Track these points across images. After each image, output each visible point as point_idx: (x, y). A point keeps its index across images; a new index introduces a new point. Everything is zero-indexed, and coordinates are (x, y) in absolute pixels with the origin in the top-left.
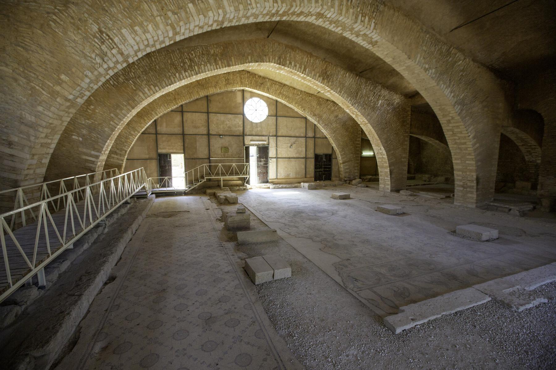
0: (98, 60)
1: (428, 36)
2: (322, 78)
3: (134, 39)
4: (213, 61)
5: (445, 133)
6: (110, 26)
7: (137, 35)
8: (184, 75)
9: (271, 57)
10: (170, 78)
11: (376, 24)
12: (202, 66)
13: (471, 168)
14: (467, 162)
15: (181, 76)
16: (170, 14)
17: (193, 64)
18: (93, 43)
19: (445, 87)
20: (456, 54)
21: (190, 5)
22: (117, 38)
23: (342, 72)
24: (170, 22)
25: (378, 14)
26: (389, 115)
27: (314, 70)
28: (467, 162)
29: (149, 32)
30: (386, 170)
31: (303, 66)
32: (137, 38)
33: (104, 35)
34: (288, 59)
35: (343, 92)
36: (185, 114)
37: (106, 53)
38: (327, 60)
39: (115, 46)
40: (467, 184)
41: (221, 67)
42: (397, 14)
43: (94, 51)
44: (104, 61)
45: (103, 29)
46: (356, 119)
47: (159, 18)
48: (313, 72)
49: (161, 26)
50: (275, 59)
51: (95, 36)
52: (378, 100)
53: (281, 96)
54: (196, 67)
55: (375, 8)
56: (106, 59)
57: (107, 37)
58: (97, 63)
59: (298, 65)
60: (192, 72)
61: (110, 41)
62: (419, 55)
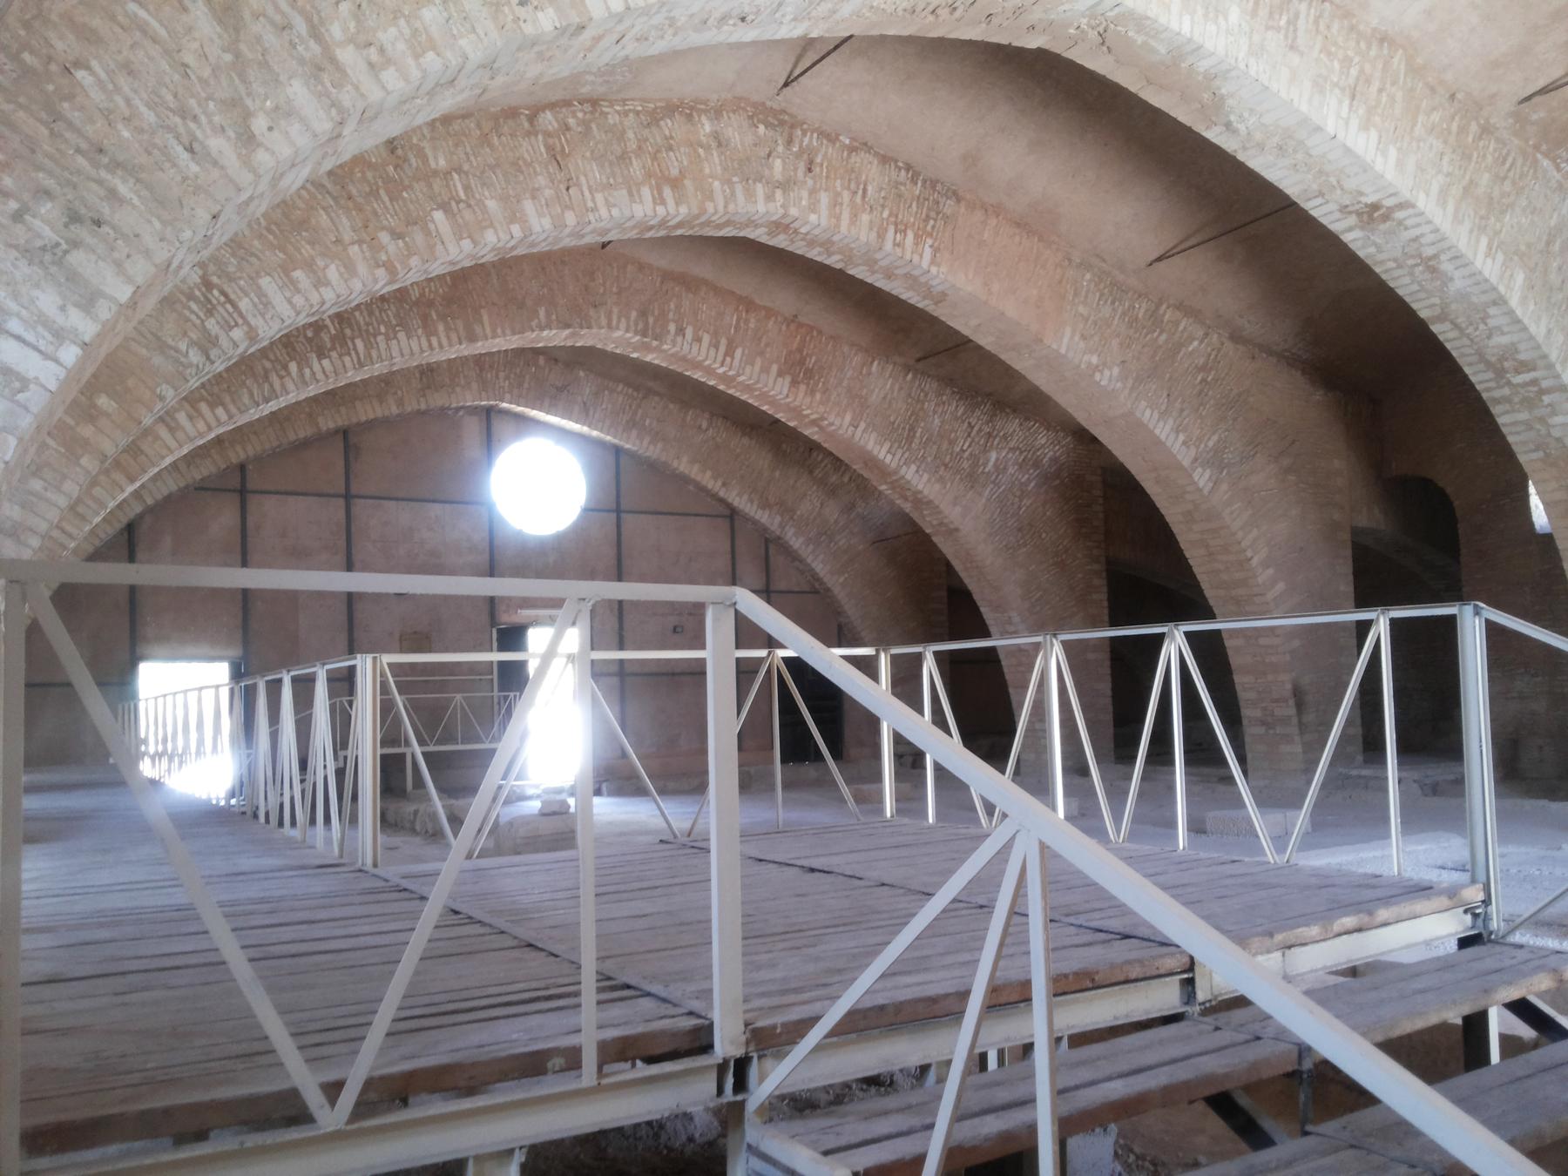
0: (195, 357)
1: (1088, 276)
2: (788, 379)
3: (289, 302)
4: (416, 322)
5: (1187, 555)
6: (231, 269)
7: (298, 291)
8: (316, 366)
9: (615, 310)
10: (266, 377)
11: (936, 250)
12: (380, 338)
15: (307, 371)
16: (384, 237)
17: (348, 332)
18: (187, 313)
19: (1156, 415)
20: (1177, 323)
21: (438, 215)
22: (246, 300)
23: (857, 359)
24: (384, 258)
25: (940, 223)
26: (1026, 502)
27: (762, 353)
29: (328, 284)
31: (724, 342)
32: (298, 300)
33: (216, 292)
34: (671, 315)
35: (862, 425)
36: (254, 502)
37: (217, 337)
38: (801, 319)
39: (240, 321)
41: (445, 341)
42: (993, 221)
43: (185, 334)
44: (208, 358)
45: (215, 280)
46: (915, 516)
47: (356, 247)
48: (758, 362)
49: (362, 269)
50: (628, 319)
51: (191, 297)
52: (985, 450)
53: (634, 433)
54: (360, 344)
55: (929, 209)
56: (213, 353)
57: (222, 299)
58: (191, 365)
59: (706, 339)
60: (347, 359)
61: (228, 306)
62: (1068, 331)
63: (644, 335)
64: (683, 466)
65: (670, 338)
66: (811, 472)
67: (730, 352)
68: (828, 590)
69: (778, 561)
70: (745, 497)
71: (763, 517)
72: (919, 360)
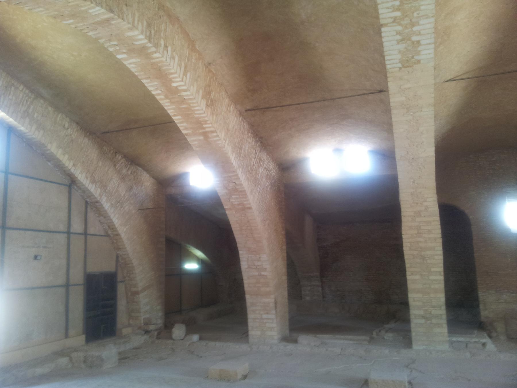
9: (137, 15)
13: (437, 286)
14: (432, 277)
23: (226, 101)
28: (432, 277)
30: (266, 300)
31: (183, 65)
40: (430, 314)
63: (150, 41)
64: (53, 149)
65: (161, 49)
66: (115, 166)
67: (185, 74)
68: (118, 235)
69: (91, 215)
70: (84, 175)
71: (93, 189)
72: (247, 110)
